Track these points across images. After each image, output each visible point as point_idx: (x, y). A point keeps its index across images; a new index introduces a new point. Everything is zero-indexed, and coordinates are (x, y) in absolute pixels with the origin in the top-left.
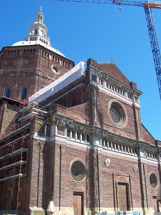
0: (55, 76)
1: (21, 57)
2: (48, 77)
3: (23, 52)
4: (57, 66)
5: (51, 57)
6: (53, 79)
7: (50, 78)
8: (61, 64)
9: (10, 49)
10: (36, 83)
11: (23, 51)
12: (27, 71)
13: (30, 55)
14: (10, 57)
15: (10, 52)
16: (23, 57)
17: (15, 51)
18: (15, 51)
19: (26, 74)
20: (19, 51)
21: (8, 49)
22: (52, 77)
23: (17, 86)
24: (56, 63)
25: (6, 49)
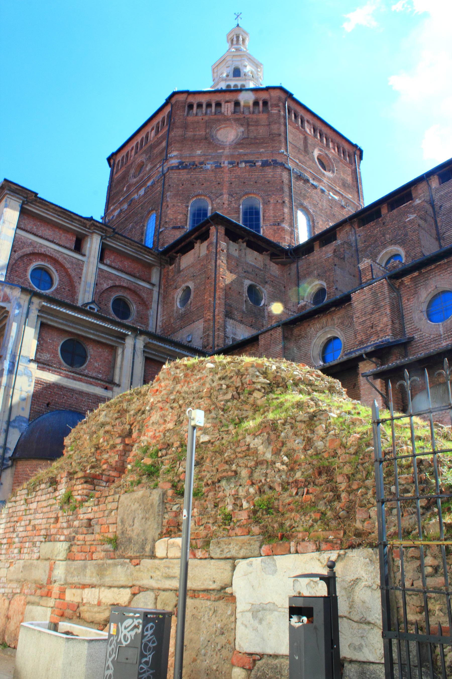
0: (325, 180)
1: (227, 120)
2: (312, 181)
3: (233, 106)
4: (326, 154)
5: (308, 130)
6: (321, 187)
7: (315, 183)
8: (333, 151)
9: (191, 99)
10: (286, 189)
11: (233, 103)
12: (251, 158)
13: (254, 116)
14: (196, 119)
15: (191, 106)
16: (237, 120)
17: (209, 105)
18: (209, 105)
19: (251, 166)
20: (218, 105)
21: (187, 99)
22: (320, 181)
23: (226, 196)
24: (323, 147)
25: (182, 98)
